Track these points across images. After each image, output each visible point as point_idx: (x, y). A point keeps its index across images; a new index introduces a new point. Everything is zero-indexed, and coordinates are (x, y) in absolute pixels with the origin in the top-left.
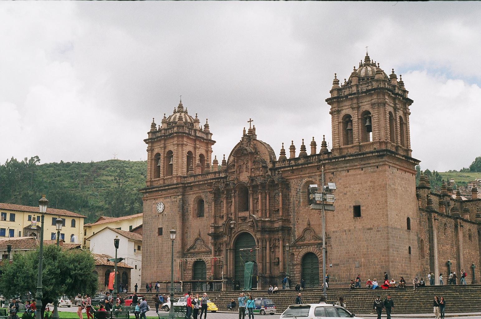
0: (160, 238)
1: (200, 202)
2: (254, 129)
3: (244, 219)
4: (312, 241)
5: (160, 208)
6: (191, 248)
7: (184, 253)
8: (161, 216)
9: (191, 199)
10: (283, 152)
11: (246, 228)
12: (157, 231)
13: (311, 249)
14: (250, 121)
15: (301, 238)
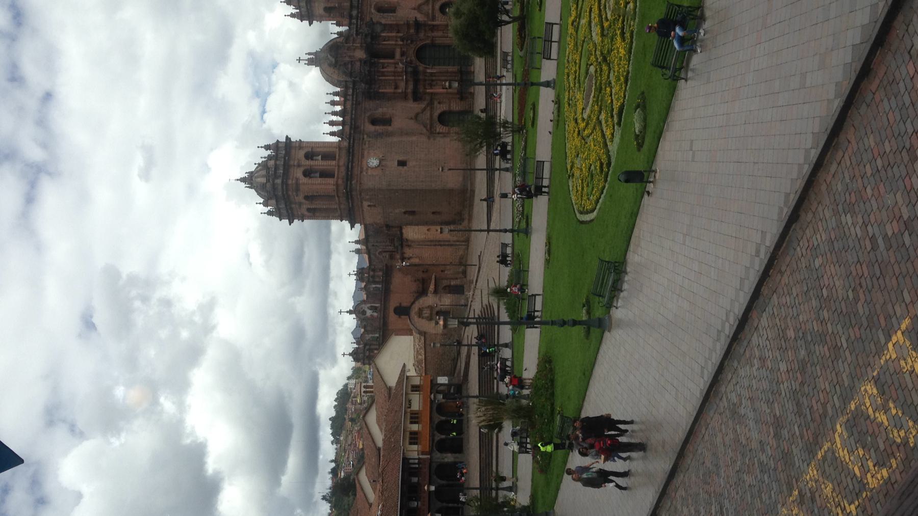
0: (410, 164)
1: (374, 122)
2: (309, 54)
3: (403, 54)
4: (430, 6)
5: (374, 162)
6: (425, 127)
7: (432, 133)
8: (383, 163)
9: (371, 128)
10: (338, 33)
11: (411, 53)
12: (401, 168)
13: (437, 6)
14: (299, 60)
15: (427, 15)
